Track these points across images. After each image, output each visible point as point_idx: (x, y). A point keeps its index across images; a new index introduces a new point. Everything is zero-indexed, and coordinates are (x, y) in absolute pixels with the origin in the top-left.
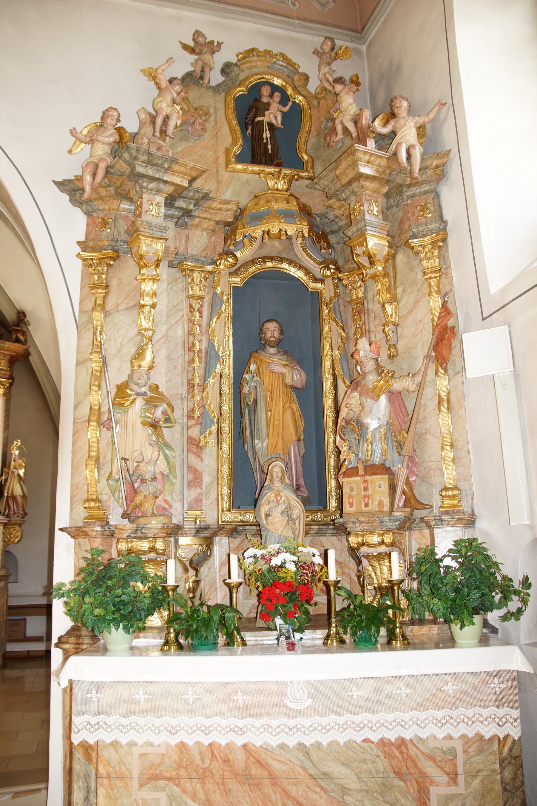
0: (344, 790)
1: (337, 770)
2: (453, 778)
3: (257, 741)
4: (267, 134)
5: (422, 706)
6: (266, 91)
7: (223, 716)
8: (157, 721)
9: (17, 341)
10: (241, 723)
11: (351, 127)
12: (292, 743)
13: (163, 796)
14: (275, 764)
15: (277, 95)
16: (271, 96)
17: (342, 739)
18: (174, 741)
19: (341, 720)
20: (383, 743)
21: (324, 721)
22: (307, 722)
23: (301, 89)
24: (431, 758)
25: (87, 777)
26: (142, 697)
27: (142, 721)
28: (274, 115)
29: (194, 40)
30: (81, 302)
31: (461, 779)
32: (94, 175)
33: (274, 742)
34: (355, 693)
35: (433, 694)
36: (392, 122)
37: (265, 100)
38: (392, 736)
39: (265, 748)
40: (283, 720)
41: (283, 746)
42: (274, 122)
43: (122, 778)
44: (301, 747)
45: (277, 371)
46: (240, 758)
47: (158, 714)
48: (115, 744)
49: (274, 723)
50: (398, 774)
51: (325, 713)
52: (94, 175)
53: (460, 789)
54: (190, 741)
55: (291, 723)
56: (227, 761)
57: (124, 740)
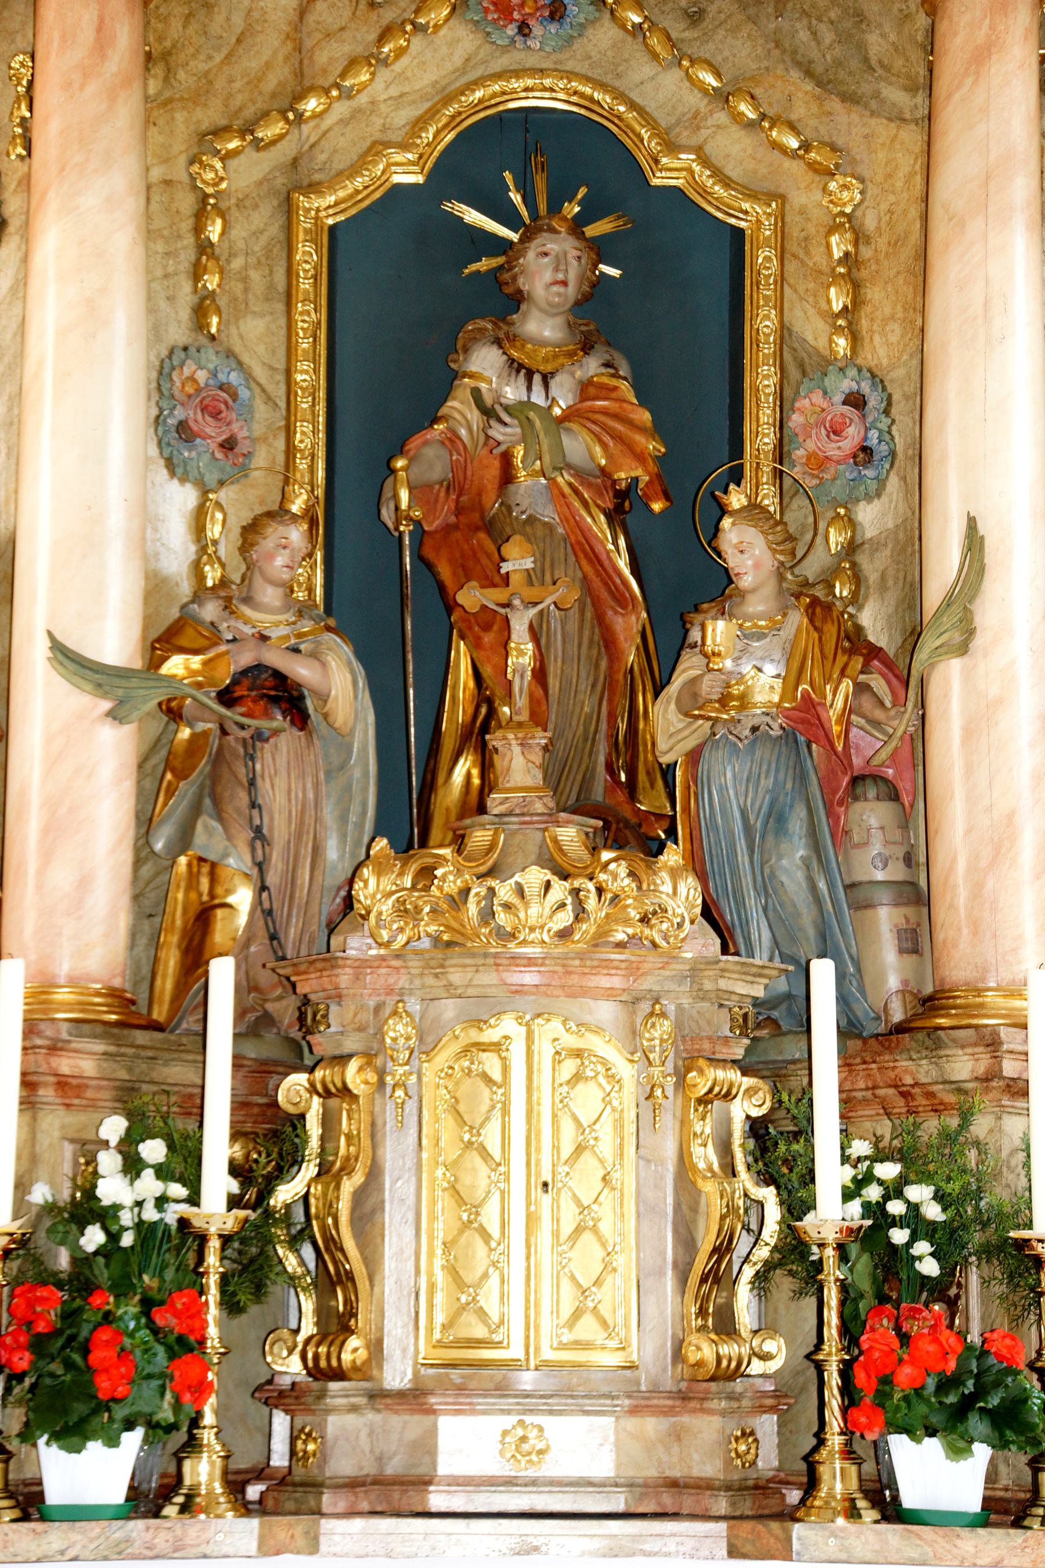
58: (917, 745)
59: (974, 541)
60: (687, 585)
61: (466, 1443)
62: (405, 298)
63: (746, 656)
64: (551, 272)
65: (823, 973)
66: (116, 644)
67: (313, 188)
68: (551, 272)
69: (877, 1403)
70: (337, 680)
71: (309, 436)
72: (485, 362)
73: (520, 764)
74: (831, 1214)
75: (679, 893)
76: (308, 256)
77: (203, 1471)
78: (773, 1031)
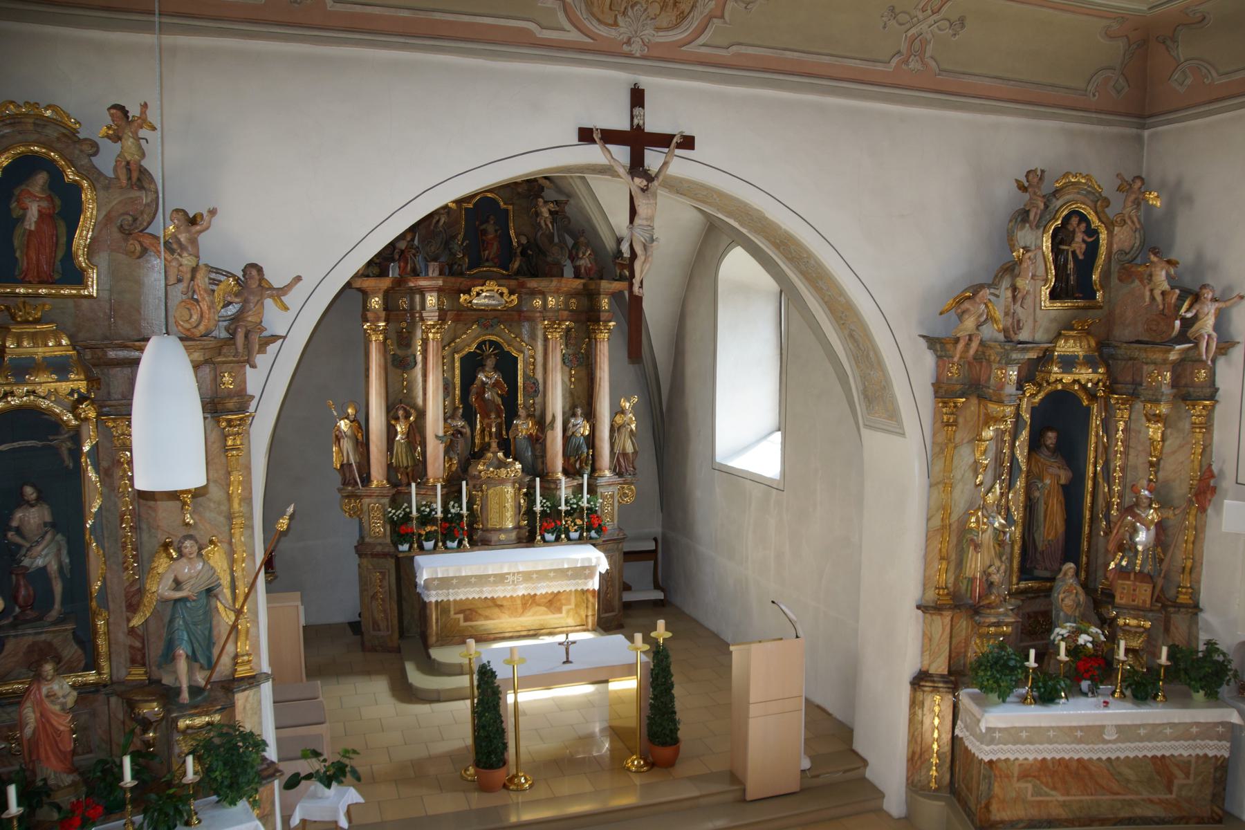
0: (1128, 781)
1: (1127, 772)
2: (1187, 776)
3: (1086, 757)
4: (1071, 265)
5: (1177, 739)
6: (1074, 221)
7: (1067, 743)
8: (1032, 747)
9: (621, 278)
10: (1078, 747)
11: (1159, 298)
12: (1104, 757)
13: (1030, 786)
14: (1093, 769)
15: (1083, 226)
16: (1079, 224)
17: (1131, 755)
18: (1040, 758)
19: (1132, 745)
20: (1154, 757)
21: (1123, 746)
22: (1114, 746)
23: (1101, 215)
24: (1177, 765)
25: (990, 777)
26: (1024, 734)
27: (1023, 747)
28: (1078, 244)
29: (1027, 176)
30: (934, 435)
31: (1192, 776)
32: (968, 345)
33: (1095, 757)
34: (1142, 732)
35: (1183, 732)
36: (1197, 307)
37: (1070, 228)
38: (1159, 754)
39: (1090, 760)
40: (1101, 746)
41: (1099, 759)
42: (1078, 252)
43: (1008, 777)
44: (1109, 759)
45: (1055, 475)
46: (1075, 764)
47: (1032, 743)
48: (1007, 760)
49: (1096, 747)
50: (1158, 773)
51: (1123, 742)
52: (968, 345)
53: (1191, 781)
54: (1049, 757)
55: (1105, 747)
56: (1067, 767)
57: (1012, 758)
58: (545, 440)
59: (554, 416)
60: (512, 413)
61: (494, 537)
62: (472, 365)
63: (524, 427)
64: (490, 363)
65: (538, 479)
66: (441, 433)
67: (457, 352)
68: (490, 363)
69: (544, 530)
70: (467, 430)
71: (458, 392)
72: (482, 377)
73: (494, 445)
74: (538, 508)
75: (518, 466)
76: (457, 364)
77: (466, 542)
78: (531, 487)
